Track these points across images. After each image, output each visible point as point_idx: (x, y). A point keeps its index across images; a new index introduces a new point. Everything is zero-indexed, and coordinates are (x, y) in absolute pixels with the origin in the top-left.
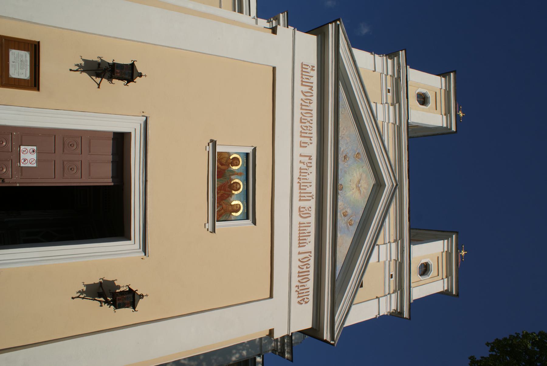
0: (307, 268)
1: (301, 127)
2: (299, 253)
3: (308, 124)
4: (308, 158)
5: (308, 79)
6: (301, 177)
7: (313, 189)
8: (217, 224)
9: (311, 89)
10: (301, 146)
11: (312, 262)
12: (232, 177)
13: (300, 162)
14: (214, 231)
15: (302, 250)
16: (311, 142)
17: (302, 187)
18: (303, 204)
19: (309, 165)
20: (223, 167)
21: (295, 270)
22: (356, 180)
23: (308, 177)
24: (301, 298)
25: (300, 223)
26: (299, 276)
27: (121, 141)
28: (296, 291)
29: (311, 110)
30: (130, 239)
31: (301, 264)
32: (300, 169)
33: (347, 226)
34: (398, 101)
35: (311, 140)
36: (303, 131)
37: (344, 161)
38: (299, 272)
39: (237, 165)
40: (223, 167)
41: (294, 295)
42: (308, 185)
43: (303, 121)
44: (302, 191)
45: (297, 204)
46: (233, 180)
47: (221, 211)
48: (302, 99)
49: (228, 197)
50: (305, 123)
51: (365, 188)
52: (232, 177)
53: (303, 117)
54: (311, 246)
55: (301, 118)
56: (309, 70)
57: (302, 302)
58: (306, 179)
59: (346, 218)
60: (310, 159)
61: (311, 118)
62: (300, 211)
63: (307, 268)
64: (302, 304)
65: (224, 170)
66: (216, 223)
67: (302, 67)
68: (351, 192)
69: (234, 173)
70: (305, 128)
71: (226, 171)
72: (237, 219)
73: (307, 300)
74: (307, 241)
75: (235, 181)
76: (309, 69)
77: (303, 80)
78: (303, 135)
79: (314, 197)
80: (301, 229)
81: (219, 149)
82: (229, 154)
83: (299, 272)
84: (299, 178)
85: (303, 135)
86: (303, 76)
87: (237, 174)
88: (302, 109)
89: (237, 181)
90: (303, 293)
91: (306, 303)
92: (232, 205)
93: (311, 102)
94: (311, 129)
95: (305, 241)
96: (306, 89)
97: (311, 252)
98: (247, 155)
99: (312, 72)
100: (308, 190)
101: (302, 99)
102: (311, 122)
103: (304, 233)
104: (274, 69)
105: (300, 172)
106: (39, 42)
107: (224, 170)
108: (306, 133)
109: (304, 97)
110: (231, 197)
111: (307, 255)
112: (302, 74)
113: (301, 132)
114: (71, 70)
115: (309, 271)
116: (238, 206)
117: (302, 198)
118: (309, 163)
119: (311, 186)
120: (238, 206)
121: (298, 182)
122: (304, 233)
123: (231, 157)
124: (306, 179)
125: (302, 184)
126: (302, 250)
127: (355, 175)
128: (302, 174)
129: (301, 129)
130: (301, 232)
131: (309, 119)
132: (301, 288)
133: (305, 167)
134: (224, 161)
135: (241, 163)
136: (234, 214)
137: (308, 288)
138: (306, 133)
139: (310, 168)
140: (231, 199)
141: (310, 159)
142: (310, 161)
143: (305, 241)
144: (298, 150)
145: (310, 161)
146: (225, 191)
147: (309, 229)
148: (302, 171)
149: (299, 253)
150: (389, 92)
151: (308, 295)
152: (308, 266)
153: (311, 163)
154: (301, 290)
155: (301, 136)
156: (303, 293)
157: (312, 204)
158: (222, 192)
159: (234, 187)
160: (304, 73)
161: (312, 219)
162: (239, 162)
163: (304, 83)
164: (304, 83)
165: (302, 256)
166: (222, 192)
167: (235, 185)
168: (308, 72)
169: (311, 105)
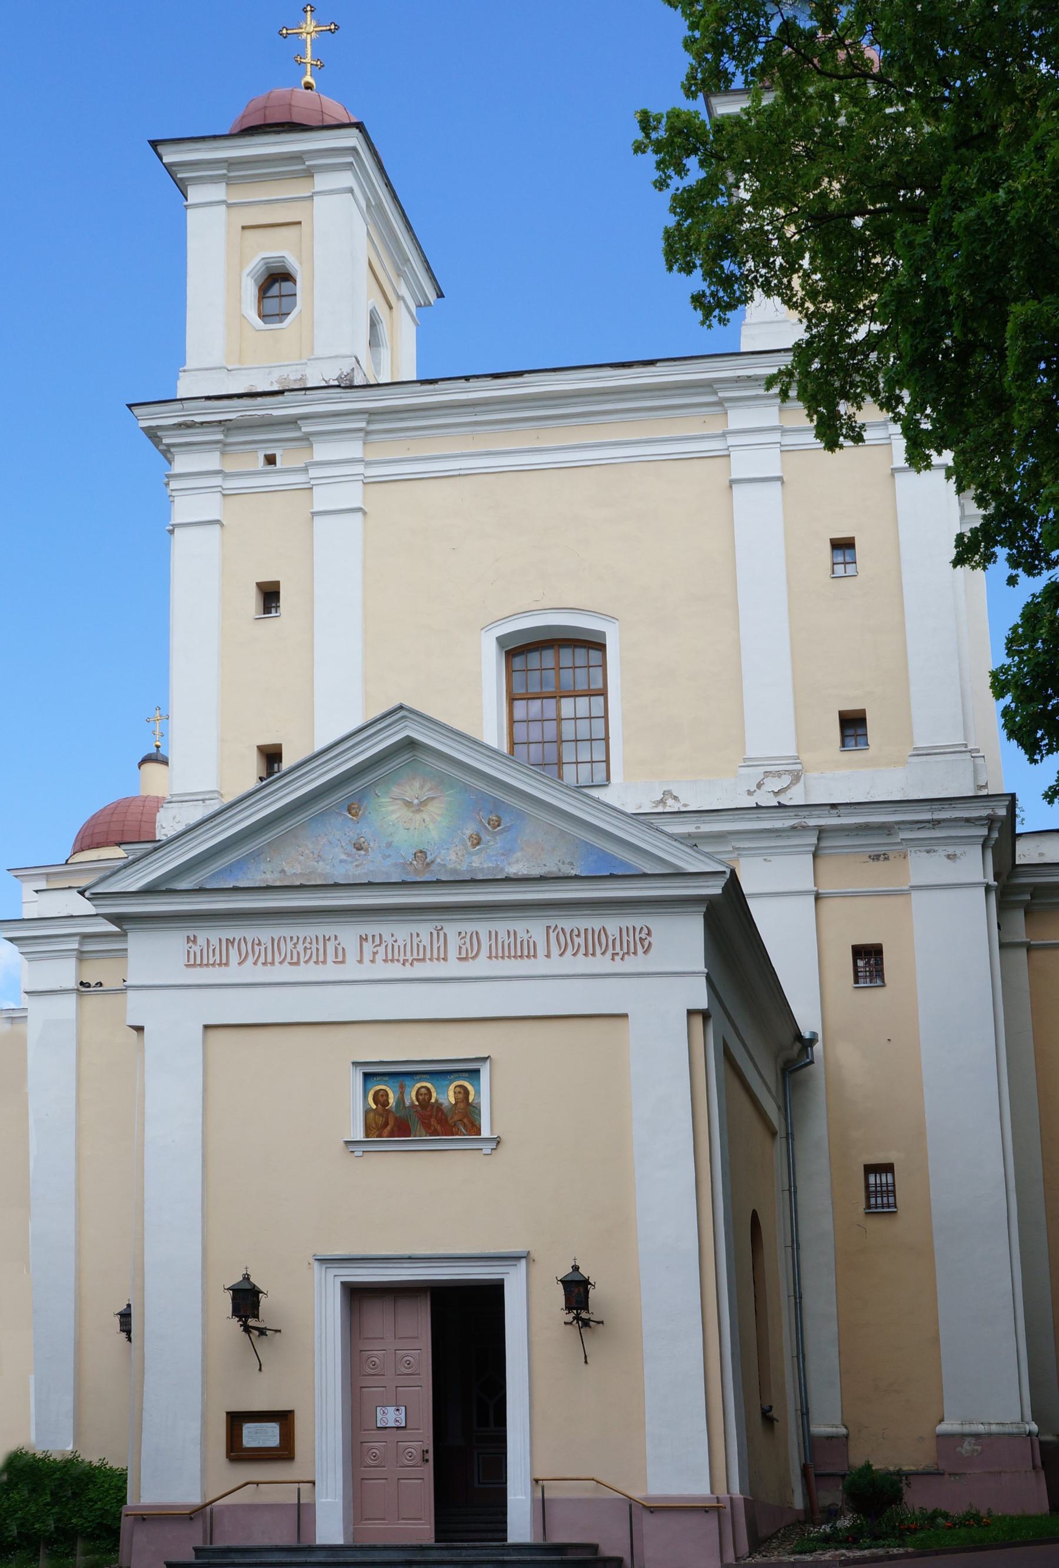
0: (578, 935)
1: (306, 962)
2: (548, 956)
3: (300, 947)
9: (233, 943)
10: (343, 962)
12: (407, 1104)
13: (373, 961)
14: (498, 1141)
15: (541, 951)
16: (333, 938)
17: (421, 957)
18: (453, 953)
19: (377, 942)
20: (391, 1122)
23: (401, 943)
24: (639, 946)
25: (490, 957)
26: (593, 954)
27: (357, 1295)
28: (622, 959)
32: (385, 961)
33: (501, 833)
35: (329, 939)
36: (314, 958)
37: (366, 850)
38: (586, 955)
39: (387, 1095)
40: (391, 1122)
42: (415, 940)
43: (295, 960)
44: (428, 955)
45: (453, 968)
46: (412, 1102)
48: (255, 963)
49: (443, 1113)
51: (422, 787)
52: (407, 1104)
54: (534, 929)
55: (291, 964)
56: (197, 949)
59: (485, 837)
60: (366, 939)
61: (288, 940)
62: (466, 959)
63: (578, 935)
64: (650, 943)
65: (396, 1118)
66: (482, 1136)
67: (194, 965)
68: (431, 826)
69: (400, 1101)
70: (309, 952)
71: (398, 1115)
72: (478, 1092)
73: (645, 931)
74: (526, 937)
77: (218, 961)
78: (321, 959)
79: (439, 925)
80: (500, 954)
84: (404, 964)
85: (321, 959)
86: (211, 962)
87: (402, 1093)
91: (649, 934)
92: (456, 1103)
93: (257, 942)
96: (233, 952)
97: (548, 928)
98: (367, 1076)
99: (200, 941)
101: (255, 963)
102: (295, 940)
103: (509, 945)
104: (206, 1027)
105: (392, 961)
106: (228, 1413)
107: (396, 1118)
108: (317, 949)
109: (251, 959)
110: (441, 1104)
112: (207, 965)
114: (260, 1370)
116: (458, 1089)
117: (442, 956)
118: (373, 942)
119: (418, 935)
121: (411, 964)
122: (509, 945)
123: (374, 1107)
125: (415, 956)
126: (541, 951)
127: (394, 817)
128: (396, 957)
130: (507, 954)
131: (290, 945)
132: (618, 949)
133: (381, 949)
134: (381, 1121)
138: (317, 949)
139: (384, 939)
140: (445, 1103)
142: (370, 939)
145: (370, 939)
146: (431, 1116)
148: (390, 957)
149: (548, 956)
152: (576, 932)
153: (373, 936)
154: (621, 949)
158: (433, 1121)
159: (424, 1100)
163: (224, 961)
164: (224, 961)
165: (555, 950)
166: (433, 1121)
167: (421, 1097)
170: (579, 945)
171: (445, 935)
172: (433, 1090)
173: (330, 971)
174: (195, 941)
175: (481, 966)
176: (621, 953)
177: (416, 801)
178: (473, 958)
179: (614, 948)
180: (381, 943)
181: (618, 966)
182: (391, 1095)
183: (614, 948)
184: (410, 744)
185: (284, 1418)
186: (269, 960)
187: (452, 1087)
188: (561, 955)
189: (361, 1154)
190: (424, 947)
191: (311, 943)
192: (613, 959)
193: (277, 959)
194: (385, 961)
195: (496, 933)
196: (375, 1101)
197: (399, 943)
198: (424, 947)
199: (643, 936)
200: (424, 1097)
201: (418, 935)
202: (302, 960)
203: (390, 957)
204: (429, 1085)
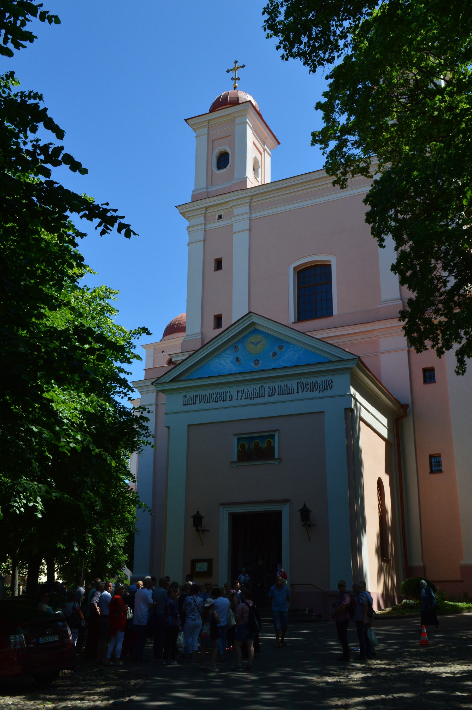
0: (308, 385)
2: (298, 393)
3: (218, 396)
7: (258, 387)
10: (232, 400)
11: (304, 381)
12: (251, 447)
13: (241, 399)
15: (296, 391)
18: (267, 394)
22: (253, 346)
25: (279, 395)
30: (281, 510)
31: (305, 390)
32: (245, 398)
38: (310, 391)
39: (245, 445)
41: (326, 393)
42: (255, 390)
48: (204, 403)
52: (251, 447)
54: (293, 384)
57: (331, 385)
67: (186, 405)
72: (274, 442)
81: (235, 459)
82: (238, 452)
83: (310, 391)
84: (251, 399)
88: (210, 402)
89: (253, 444)
91: (332, 382)
96: (198, 399)
97: (298, 383)
99: (188, 397)
101: (204, 403)
104: (189, 426)
109: (203, 401)
111: (299, 385)
112: (190, 404)
113: (223, 401)
115: (310, 383)
126: (296, 391)
129: (222, 401)
131: (215, 396)
133: (244, 395)
136: (272, 445)
137: (322, 381)
144: (234, 402)
147: (283, 386)
149: (298, 393)
150: (220, 217)
155: (226, 401)
161: (276, 385)
165: (300, 390)
173: (228, 403)
174: (186, 397)
175: (276, 398)
181: (322, 394)
182: (246, 445)
184: (253, 323)
185: (210, 562)
192: (319, 392)
193: (211, 401)
194: (245, 398)
196: (241, 448)
199: (330, 383)
204: (258, 441)
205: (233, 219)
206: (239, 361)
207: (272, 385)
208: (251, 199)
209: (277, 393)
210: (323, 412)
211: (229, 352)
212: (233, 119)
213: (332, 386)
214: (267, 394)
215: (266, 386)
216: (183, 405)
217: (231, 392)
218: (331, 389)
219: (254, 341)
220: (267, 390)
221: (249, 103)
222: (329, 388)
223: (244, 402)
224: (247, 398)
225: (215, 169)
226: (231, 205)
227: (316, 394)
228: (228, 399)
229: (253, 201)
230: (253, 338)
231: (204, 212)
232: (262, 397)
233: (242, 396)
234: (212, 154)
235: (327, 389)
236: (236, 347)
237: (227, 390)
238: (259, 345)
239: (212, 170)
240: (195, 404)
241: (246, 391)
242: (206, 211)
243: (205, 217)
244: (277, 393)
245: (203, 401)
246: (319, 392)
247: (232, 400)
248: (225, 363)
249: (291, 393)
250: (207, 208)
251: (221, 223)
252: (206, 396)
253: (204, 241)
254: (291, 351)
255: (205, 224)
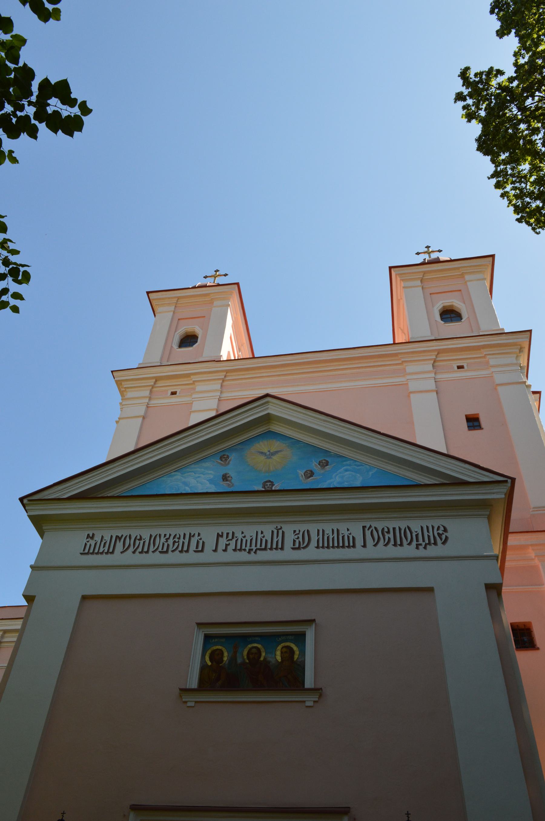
0: (388, 532)
1: (173, 551)
2: (364, 546)
3: (171, 542)
4: (220, 538)
5: (105, 543)
6: (247, 549)
7: (267, 530)
8: (309, 683)
9: (120, 539)
10: (202, 551)
12: (239, 661)
13: (225, 550)
15: (359, 542)
16: (197, 535)
17: (263, 547)
18: (288, 543)
19: (230, 537)
21: (392, 551)
22: (262, 458)
25: (318, 547)
29: (151, 536)
32: (235, 550)
34: (188, 376)
36: (180, 549)
38: (395, 545)
41: (432, 551)
42: (260, 536)
43: (165, 549)
45: (288, 554)
46: (244, 659)
47: (287, 677)
48: (134, 552)
50: (168, 545)
52: (239, 661)
53: (160, 549)
54: (354, 528)
55: (160, 552)
56: (93, 543)
57: (444, 537)
58: (251, 540)
60: (222, 536)
61: (163, 536)
62: (299, 548)
64: (447, 538)
67: (88, 553)
69: (233, 659)
70: (176, 544)
72: (303, 653)
74: (346, 534)
75: (245, 657)
76: (93, 543)
77: (106, 551)
78: (185, 548)
82: (203, 668)
83: (395, 545)
84: (249, 552)
86: (101, 551)
87: (235, 653)
89: (245, 653)
90: (429, 536)
91: (445, 530)
94: (178, 536)
95: (346, 538)
96: (120, 545)
97: (364, 527)
98: (207, 638)
99: (98, 538)
100: (268, 537)
101: (134, 552)
102: (168, 536)
103: (333, 539)
104: (84, 598)
109: (131, 549)
110: (269, 662)
111: (368, 533)
112: (97, 553)
115: (394, 529)
116: (285, 650)
118: (227, 537)
119: (262, 533)
120: (285, 650)
121: (255, 552)
122: (333, 539)
124: (251, 540)
126: (359, 542)
128: (244, 547)
129: (177, 552)
131: (163, 540)
135: (220, 647)
136: (296, 657)
137: (422, 528)
138: (183, 543)
139: (235, 535)
140: (273, 661)
141: (222, 536)
143: (346, 538)
144: (208, 556)
145: (225, 536)
147: (328, 531)
148: (239, 547)
149: (364, 546)
151: (433, 527)
152: (386, 530)
153: (228, 534)
154: (424, 541)
156: (429, 536)
157: (290, 530)
160: (96, 551)
161: (313, 529)
162: (217, 649)
163: (111, 550)
164: (111, 550)
167: (251, 656)
168: (96, 544)
169: (143, 537)
170: (389, 538)
171: (283, 533)
172: (262, 650)
173: (192, 557)
174: (92, 538)
175: (311, 553)
176: (424, 544)
177: (268, 453)
178: (304, 548)
179: (417, 540)
180: (233, 537)
181: (422, 552)
182: (226, 654)
183: (417, 540)
184: (268, 419)
186: (145, 550)
187: (279, 647)
188: (375, 545)
189: (192, 704)
190: (266, 541)
191: (179, 538)
192: (417, 548)
193: (152, 549)
194: (235, 550)
195: (323, 531)
196: (211, 659)
197: (246, 538)
198: (266, 541)
199: (441, 532)
200: (255, 654)
201: (262, 533)
202: (171, 549)
203: (239, 547)
204: (259, 646)
205: (194, 396)
206: (230, 481)
207: (303, 527)
208: (225, 376)
209: (314, 543)
210: (430, 590)
211: (207, 464)
212: (211, 302)
213: (447, 538)
214: (288, 543)
215: (289, 530)
216: (81, 554)
217: (201, 536)
218: (444, 543)
219: (265, 450)
220: (289, 538)
221: (236, 286)
222: (439, 541)
223: (231, 556)
224: (240, 550)
225: (175, 346)
226: (193, 380)
227: (409, 550)
228: (193, 546)
229: (227, 378)
230: (264, 446)
231: (153, 384)
232: (276, 549)
233: (227, 545)
234: (175, 331)
235: (435, 543)
236: (224, 458)
237: (194, 530)
238: (275, 457)
239: (172, 347)
240: (112, 553)
241: (240, 536)
242: (155, 383)
243: (151, 391)
244: (314, 543)
245: (131, 549)
246: (417, 548)
247: (202, 551)
248: (201, 478)
249: (349, 547)
250: (157, 379)
251: (174, 400)
252: (140, 539)
253: (144, 418)
254: (347, 470)
255: (150, 399)
